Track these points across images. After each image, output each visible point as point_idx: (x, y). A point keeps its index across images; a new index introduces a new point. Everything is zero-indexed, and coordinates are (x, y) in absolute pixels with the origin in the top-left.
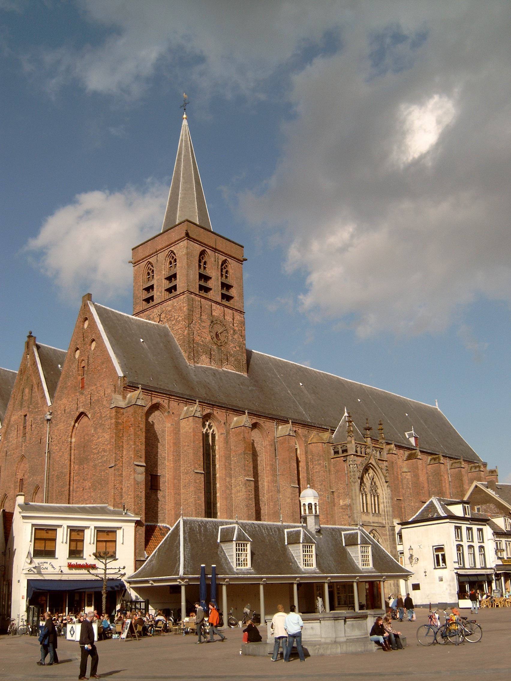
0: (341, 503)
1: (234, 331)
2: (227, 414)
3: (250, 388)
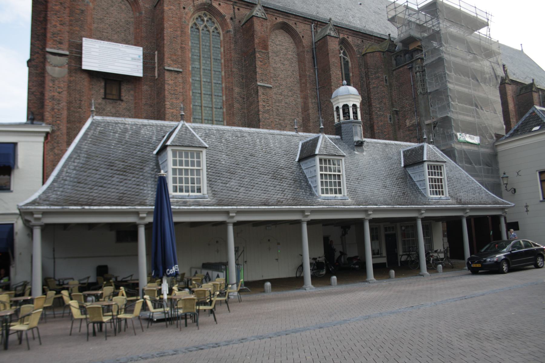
0: (408, 123)
2: (236, 8)
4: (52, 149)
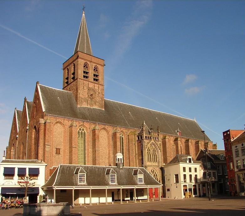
1: (99, 93)
3: (104, 115)
4: (47, 169)
